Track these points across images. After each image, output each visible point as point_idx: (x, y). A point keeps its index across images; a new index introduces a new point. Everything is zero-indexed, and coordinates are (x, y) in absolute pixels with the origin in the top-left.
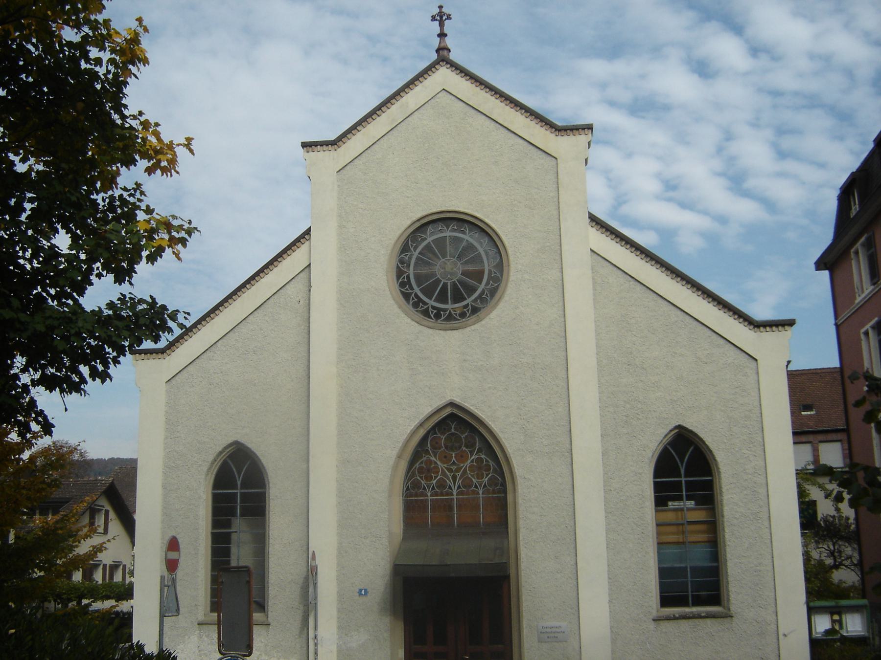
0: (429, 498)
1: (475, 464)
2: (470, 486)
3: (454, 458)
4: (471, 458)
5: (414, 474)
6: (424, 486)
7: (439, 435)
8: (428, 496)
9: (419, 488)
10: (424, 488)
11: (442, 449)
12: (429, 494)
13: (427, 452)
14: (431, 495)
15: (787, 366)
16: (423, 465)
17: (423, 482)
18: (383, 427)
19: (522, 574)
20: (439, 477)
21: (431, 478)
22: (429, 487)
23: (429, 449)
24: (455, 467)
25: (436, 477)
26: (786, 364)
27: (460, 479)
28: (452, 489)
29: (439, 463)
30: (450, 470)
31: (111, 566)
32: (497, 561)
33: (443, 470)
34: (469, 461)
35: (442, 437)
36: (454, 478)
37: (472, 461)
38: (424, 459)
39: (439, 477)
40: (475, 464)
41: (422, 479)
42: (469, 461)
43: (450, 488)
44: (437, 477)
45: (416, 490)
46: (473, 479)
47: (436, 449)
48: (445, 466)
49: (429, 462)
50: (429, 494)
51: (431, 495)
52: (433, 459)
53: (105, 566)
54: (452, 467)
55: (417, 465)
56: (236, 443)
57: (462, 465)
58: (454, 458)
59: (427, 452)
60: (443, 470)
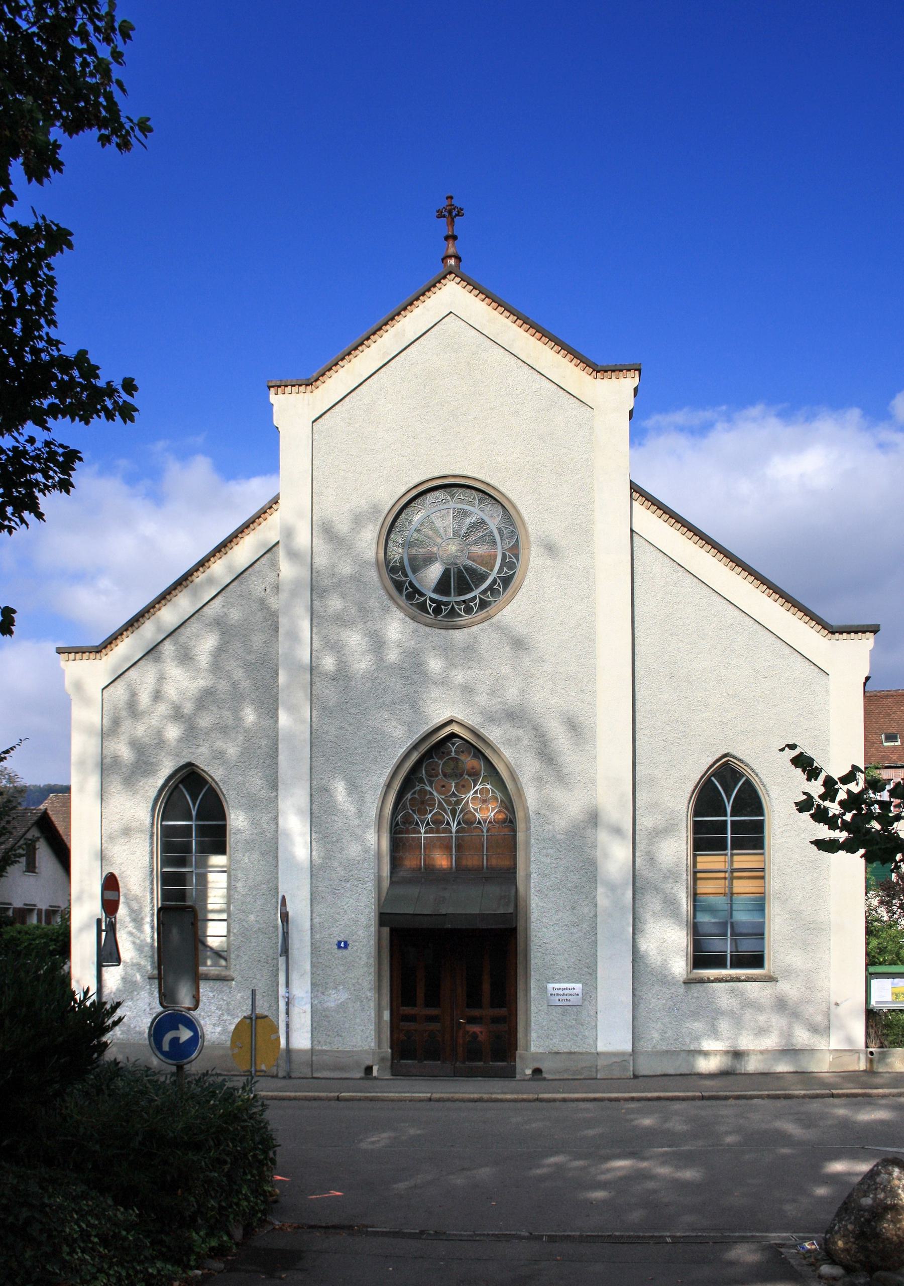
0: (423, 835)
1: (479, 795)
2: (472, 823)
3: (453, 788)
4: (474, 787)
5: (404, 807)
6: (417, 822)
7: (436, 760)
8: (421, 833)
9: (411, 823)
10: (417, 824)
11: (440, 777)
12: (423, 831)
13: (421, 781)
14: (425, 833)
15: (865, 684)
16: (416, 796)
17: (415, 817)
18: (368, 748)
19: (532, 927)
20: (435, 811)
21: (425, 813)
22: (422, 823)
23: (424, 777)
24: (455, 799)
25: (431, 811)
26: (864, 680)
27: (460, 813)
28: (450, 826)
29: (435, 794)
30: (449, 803)
31: (47, 911)
32: (501, 911)
33: (440, 802)
34: (472, 792)
35: (440, 762)
36: (454, 812)
37: (476, 792)
38: (418, 788)
39: (435, 811)
40: (479, 795)
41: (415, 813)
42: (472, 792)
43: (448, 823)
44: (433, 809)
45: (407, 825)
46: (476, 814)
47: (431, 776)
48: (443, 797)
49: (423, 792)
50: (423, 831)
51: (425, 833)
52: (428, 788)
53: (40, 911)
54: (451, 799)
55: (409, 796)
56: (190, 765)
57: (464, 796)
58: (453, 788)
59: (421, 781)
60: (440, 802)
